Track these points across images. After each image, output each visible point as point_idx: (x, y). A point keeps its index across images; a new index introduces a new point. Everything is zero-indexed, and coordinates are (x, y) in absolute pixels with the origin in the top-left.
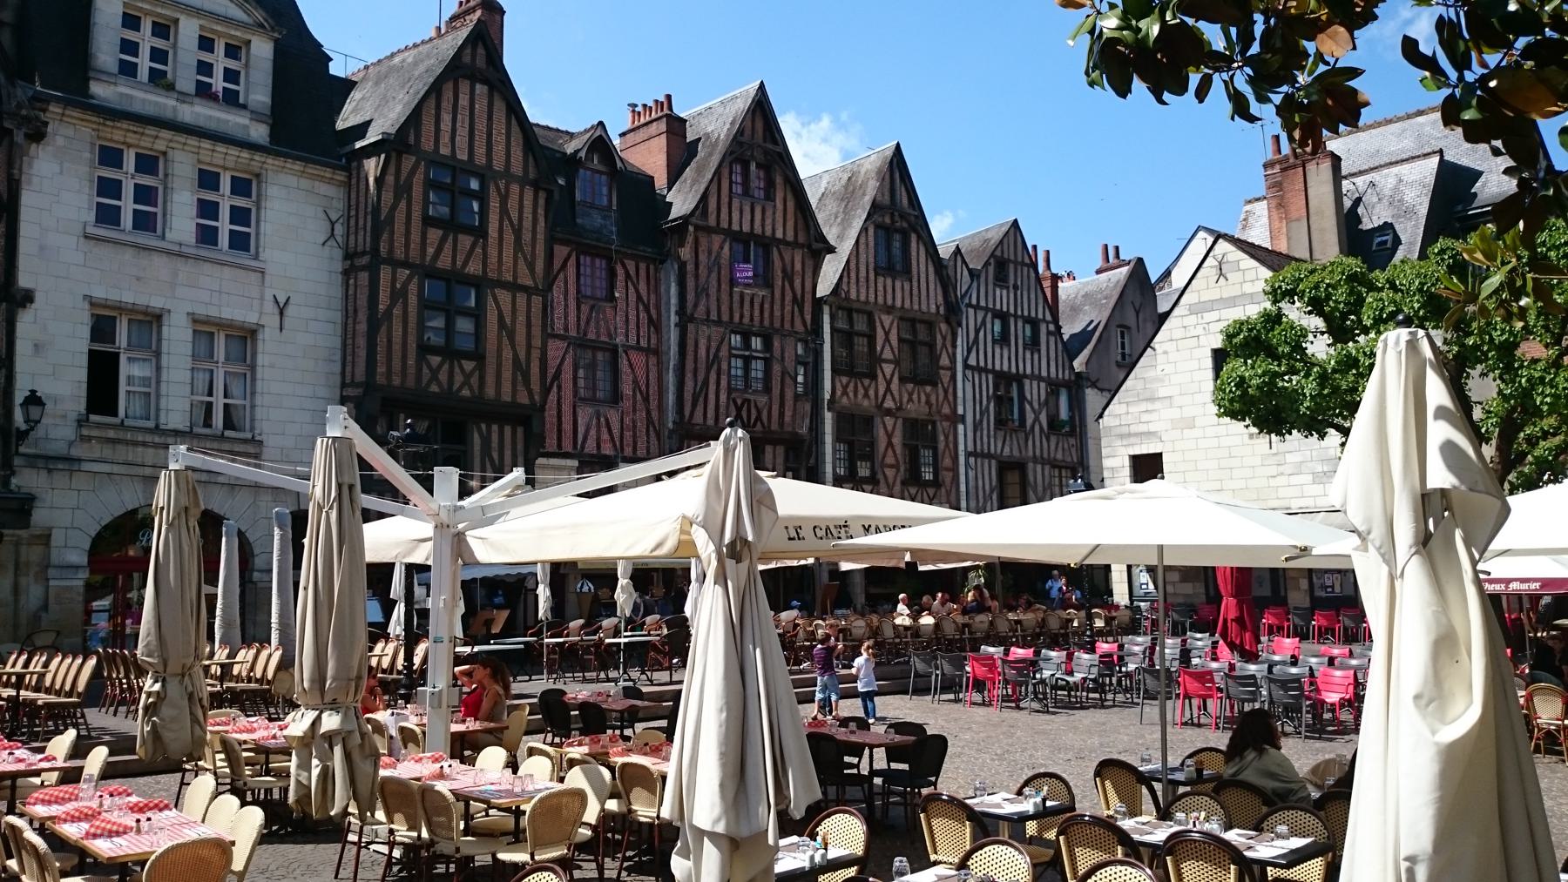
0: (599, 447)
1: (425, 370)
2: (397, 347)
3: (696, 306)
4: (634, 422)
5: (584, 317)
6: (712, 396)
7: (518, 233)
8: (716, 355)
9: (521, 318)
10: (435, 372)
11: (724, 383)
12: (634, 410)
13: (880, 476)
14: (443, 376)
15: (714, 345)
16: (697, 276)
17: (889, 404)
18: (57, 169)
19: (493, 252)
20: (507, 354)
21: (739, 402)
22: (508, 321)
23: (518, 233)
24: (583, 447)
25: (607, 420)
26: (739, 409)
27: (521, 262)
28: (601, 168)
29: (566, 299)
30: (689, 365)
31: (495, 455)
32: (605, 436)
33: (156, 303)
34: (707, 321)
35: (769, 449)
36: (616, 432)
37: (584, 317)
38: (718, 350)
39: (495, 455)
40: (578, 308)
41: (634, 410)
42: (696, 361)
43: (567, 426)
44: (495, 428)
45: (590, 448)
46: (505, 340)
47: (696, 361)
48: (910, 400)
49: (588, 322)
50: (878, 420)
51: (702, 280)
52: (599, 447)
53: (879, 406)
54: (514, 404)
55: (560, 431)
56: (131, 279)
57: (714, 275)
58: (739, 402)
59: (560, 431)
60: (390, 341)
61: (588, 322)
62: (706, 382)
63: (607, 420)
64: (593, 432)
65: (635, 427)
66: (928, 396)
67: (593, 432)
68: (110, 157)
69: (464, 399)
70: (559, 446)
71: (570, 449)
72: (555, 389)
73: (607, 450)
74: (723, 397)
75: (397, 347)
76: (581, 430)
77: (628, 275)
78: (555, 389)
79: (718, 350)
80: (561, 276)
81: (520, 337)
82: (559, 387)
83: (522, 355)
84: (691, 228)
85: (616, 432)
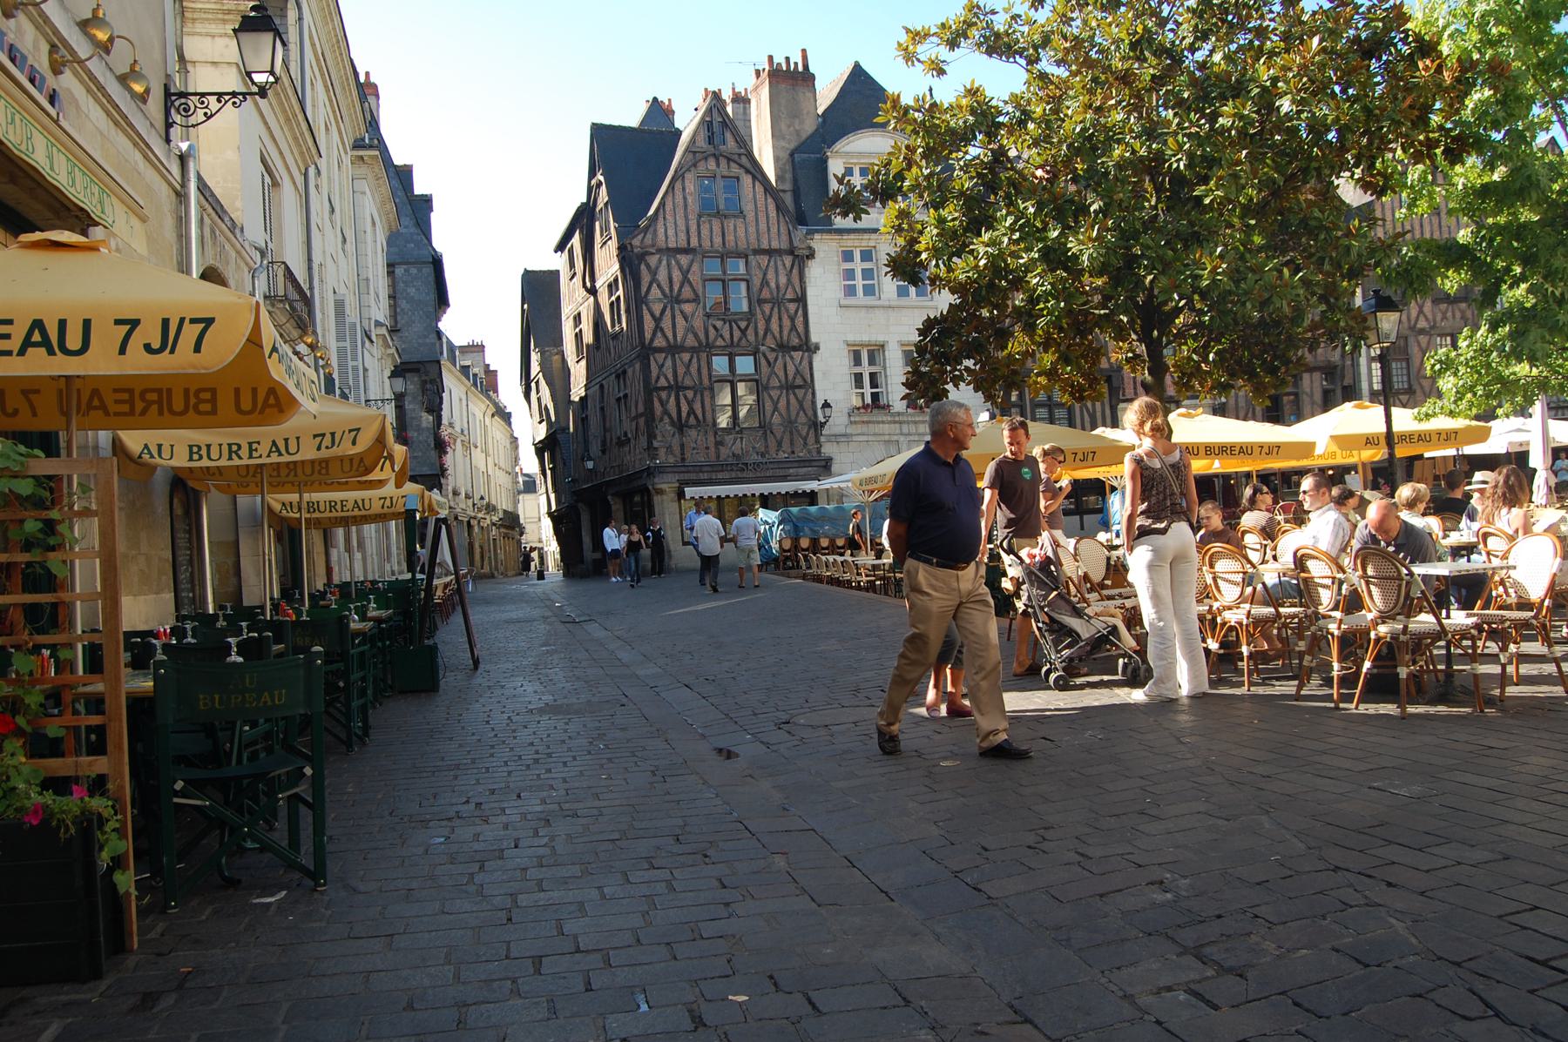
13: (1416, 386)
17: (1422, 324)
33: (881, 339)
35: (1306, 376)
48: (1444, 318)
50: (1411, 340)
53: (1412, 328)
56: (868, 330)
66: (1463, 312)
68: (848, 256)
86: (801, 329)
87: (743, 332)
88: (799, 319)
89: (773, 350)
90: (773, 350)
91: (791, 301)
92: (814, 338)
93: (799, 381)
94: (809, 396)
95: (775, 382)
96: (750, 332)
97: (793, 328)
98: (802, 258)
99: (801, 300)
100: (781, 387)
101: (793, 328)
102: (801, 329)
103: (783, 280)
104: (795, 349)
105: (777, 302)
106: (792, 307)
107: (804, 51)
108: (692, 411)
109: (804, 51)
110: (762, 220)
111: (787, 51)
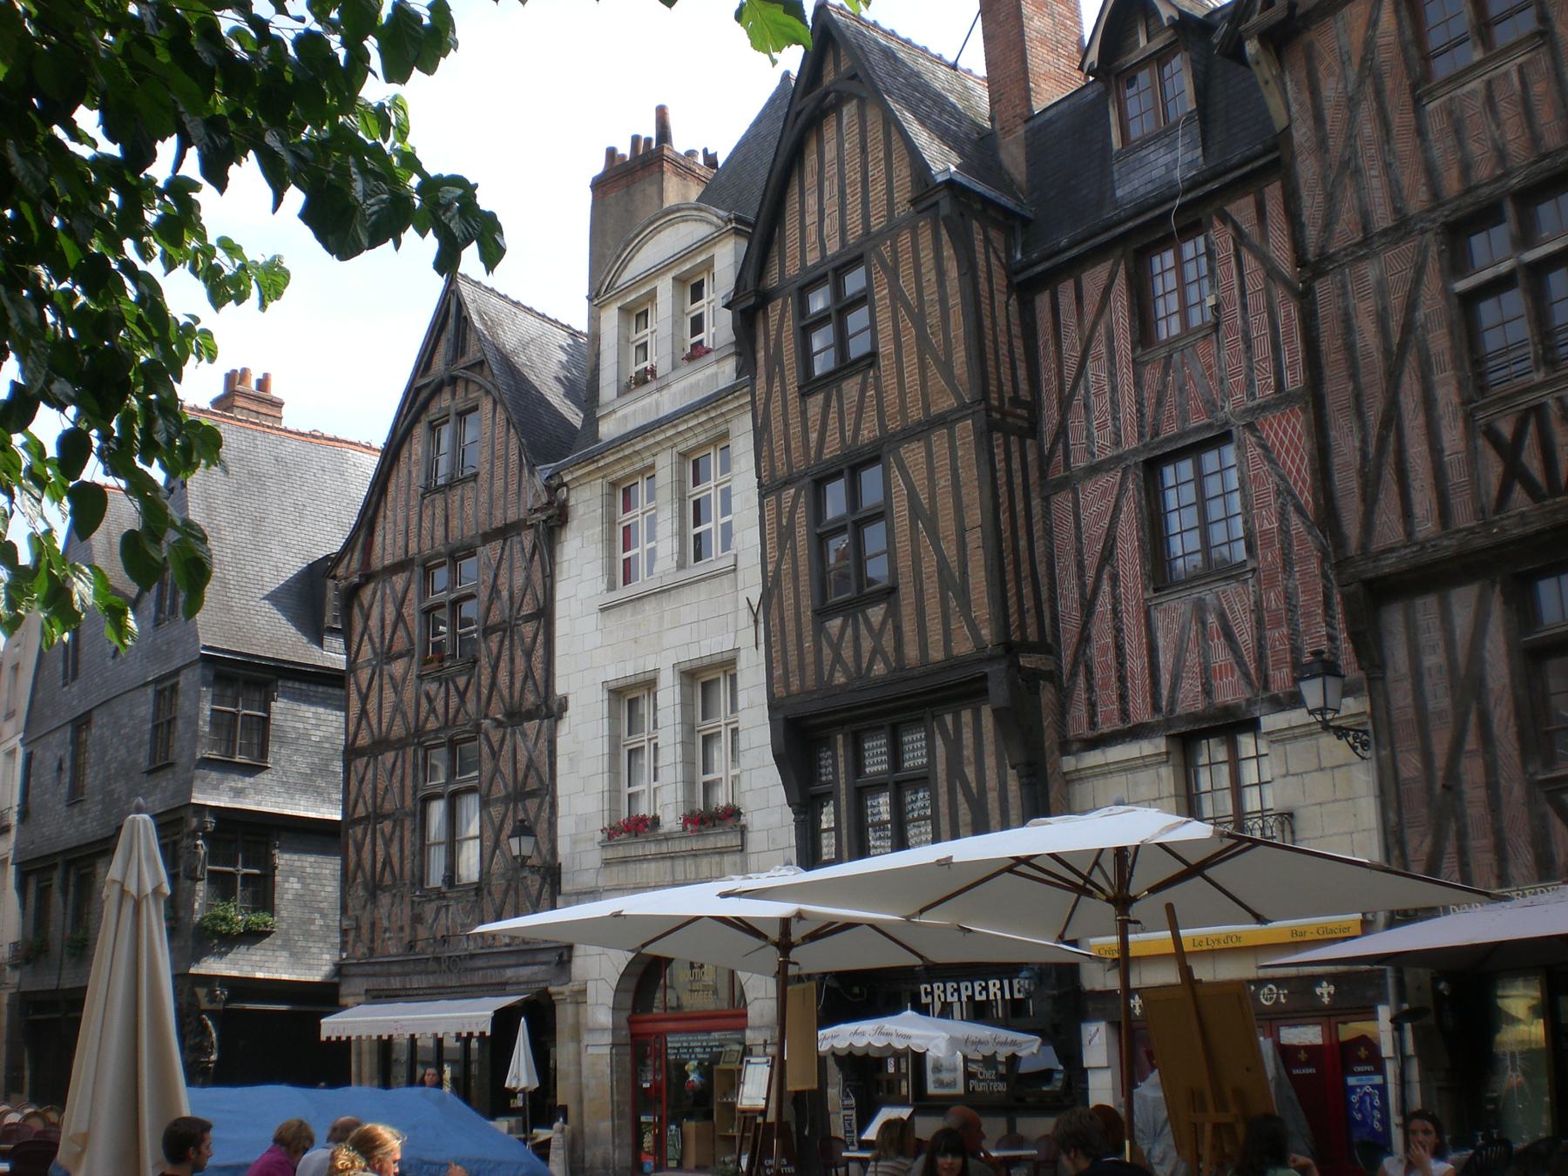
0: (1207, 691)
1: (826, 651)
2: (790, 626)
3: (1328, 225)
4: (1289, 597)
5: (1149, 395)
6: (1417, 451)
7: (919, 320)
8: (1408, 327)
9: (944, 482)
10: (836, 649)
11: (1447, 394)
12: (1287, 565)
14: (847, 653)
15: (1396, 301)
16: (1322, 145)
18: (579, 540)
19: (889, 382)
20: (929, 566)
21: (1506, 428)
22: (924, 498)
23: (919, 320)
24: (1172, 701)
25: (1222, 616)
26: (1510, 453)
27: (933, 371)
28: (1158, 43)
29: (1112, 375)
30: (1337, 390)
31: (970, 772)
32: (1220, 655)
34: (1368, 242)
36: (1245, 638)
37: (1149, 395)
38: (1411, 305)
39: (970, 772)
40: (1138, 384)
41: (1287, 565)
42: (1354, 376)
43: (1136, 664)
44: (967, 716)
45: (1190, 699)
46: (925, 540)
47: (1354, 376)
49: (1159, 403)
51: (1336, 144)
52: (1207, 691)
54: (952, 663)
55: (1122, 679)
57: (1367, 110)
58: (1506, 428)
59: (1122, 679)
60: (782, 619)
61: (1159, 403)
62: (1392, 418)
63: (1222, 616)
64: (1192, 659)
65: (1291, 608)
67: (1192, 659)
69: (884, 683)
70: (1124, 714)
71: (1147, 718)
72: (1106, 587)
73: (1230, 691)
74: (1452, 437)
75: (790, 626)
76: (1165, 660)
77: (1240, 237)
78: (1106, 587)
79: (1411, 305)
80: (1101, 329)
81: (947, 524)
82: (1114, 579)
83: (951, 552)
84: (1251, 47)
85: (1245, 638)
86: (539, 673)
87: (462, 695)
88: (540, 651)
89: (499, 724)
90: (499, 724)
91: (528, 618)
92: (560, 689)
93: (532, 784)
94: (545, 814)
95: (499, 790)
96: (471, 695)
97: (529, 674)
98: (555, 519)
99: (545, 614)
100: (507, 799)
101: (529, 674)
102: (539, 673)
103: (519, 580)
104: (530, 716)
105: (507, 628)
106: (528, 629)
107: (661, 113)
108: (387, 862)
109: (661, 113)
110: (499, 472)
111: (626, 128)
